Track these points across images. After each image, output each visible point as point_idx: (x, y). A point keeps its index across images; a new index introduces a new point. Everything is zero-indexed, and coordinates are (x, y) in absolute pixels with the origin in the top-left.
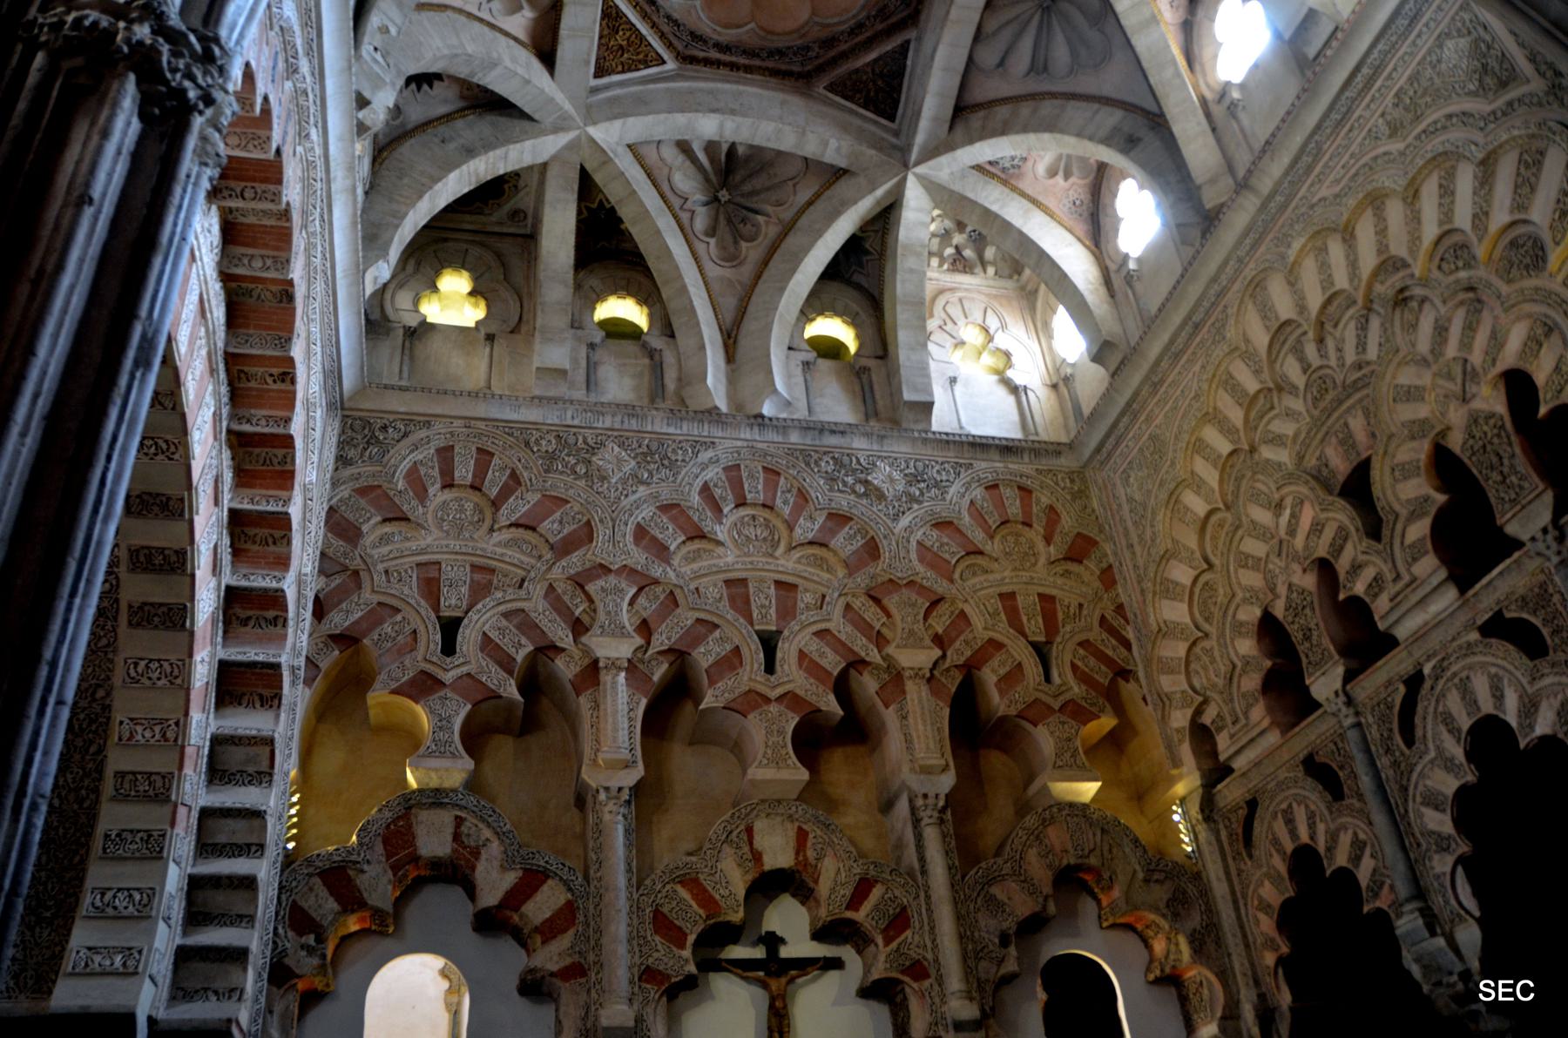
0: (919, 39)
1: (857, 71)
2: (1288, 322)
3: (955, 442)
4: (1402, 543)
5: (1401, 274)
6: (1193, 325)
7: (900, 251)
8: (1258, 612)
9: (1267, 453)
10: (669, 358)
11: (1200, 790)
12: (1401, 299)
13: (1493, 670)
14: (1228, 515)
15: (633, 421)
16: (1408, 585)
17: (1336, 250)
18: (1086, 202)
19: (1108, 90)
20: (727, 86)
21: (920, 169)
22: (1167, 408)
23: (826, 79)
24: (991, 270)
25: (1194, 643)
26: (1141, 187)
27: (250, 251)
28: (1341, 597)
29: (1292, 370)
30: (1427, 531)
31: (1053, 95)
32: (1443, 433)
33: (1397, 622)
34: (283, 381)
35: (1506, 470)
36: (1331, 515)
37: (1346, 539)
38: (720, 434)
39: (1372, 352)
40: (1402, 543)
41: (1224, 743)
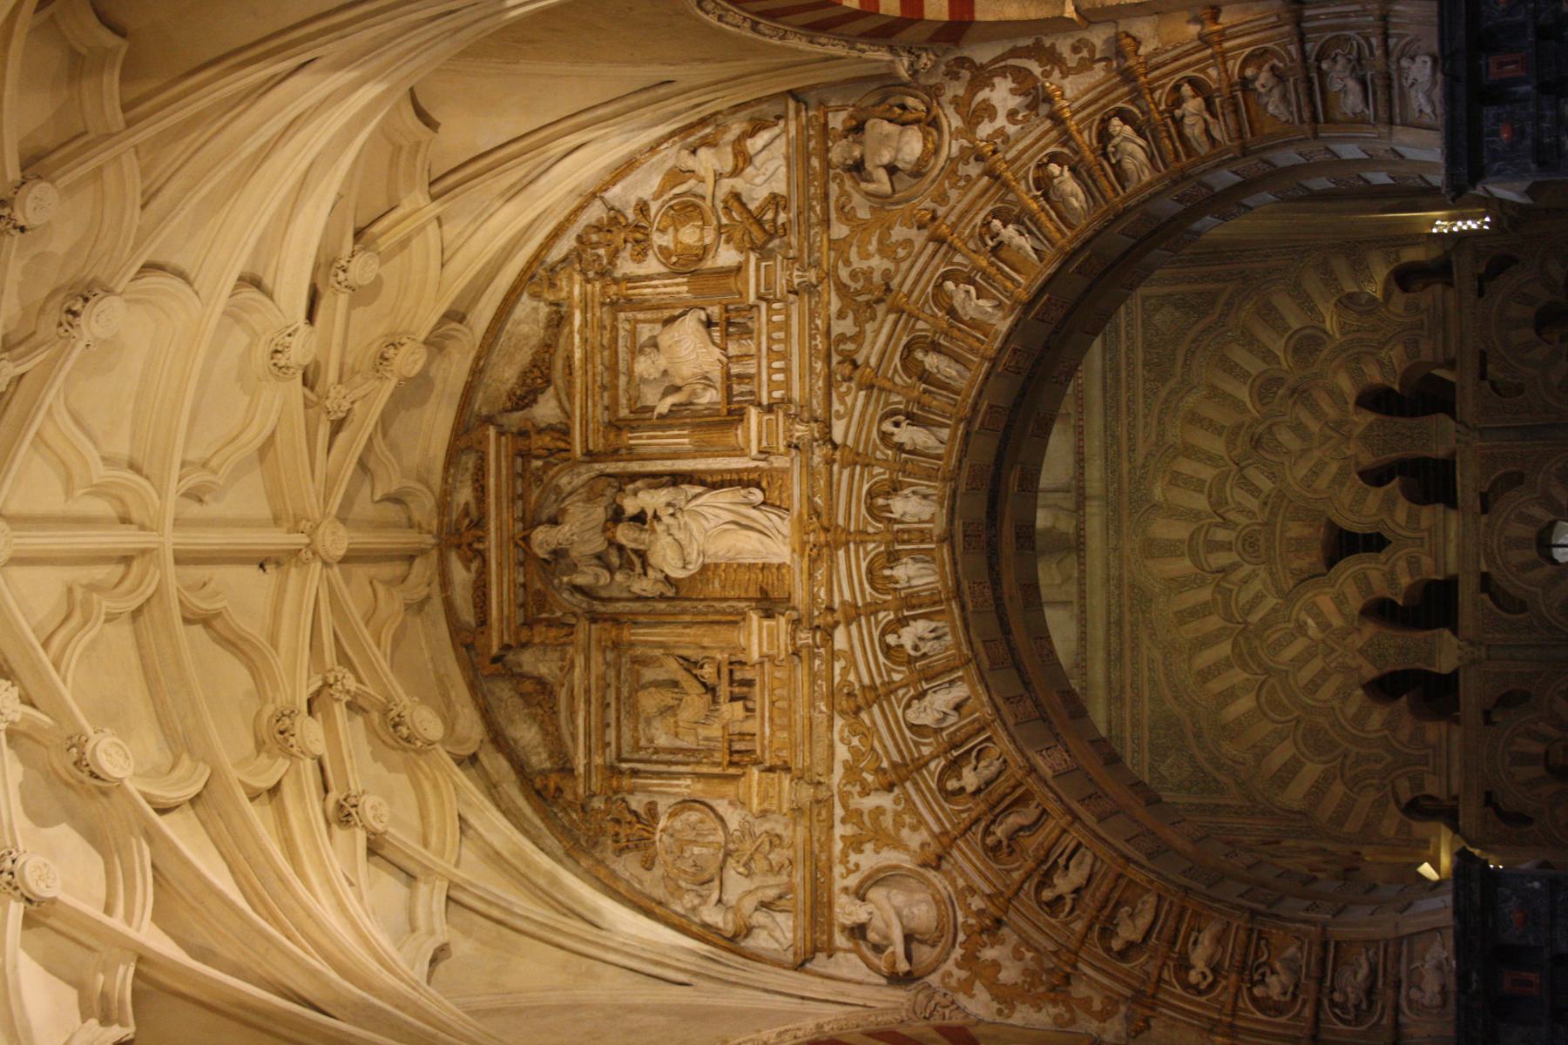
2: (1191, 538)
4: (1400, 527)
5: (1242, 433)
6: (1115, 624)
8: (1360, 692)
9: (1254, 618)
11: (1457, 837)
12: (1256, 443)
13: (1512, 517)
14: (1271, 681)
16: (1430, 535)
17: (1186, 467)
22: (1147, 694)
25: (1342, 776)
28: (1400, 602)
29: (1223, 559)
30: (1407, 504)
32: (1357, 464)
33: (1445, 564)
35: (1409, 433)
36: (1340, 581)
37: (1366, 577)
39: (1266, 485)
40: (1400, 527)
41: (1432, 787)
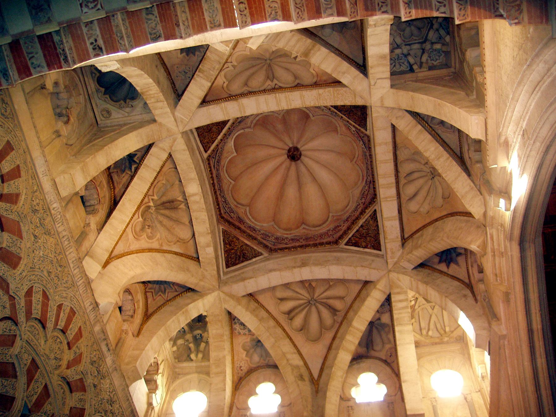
0: (267, 259)
1: (238, 239)
3: (130, 403)
7: (184, 310)
10: (92, 236)
15: (66, 243)
18: (244, 371)
19: (304, 351)
20: (208, 186)
21: (222, 295)
23: (226, 227)
24: (175, 348)
26: (276, 392)
27: (187, 10)
31: (284, 330)
34: (94, 49)
38: (81, 292)
